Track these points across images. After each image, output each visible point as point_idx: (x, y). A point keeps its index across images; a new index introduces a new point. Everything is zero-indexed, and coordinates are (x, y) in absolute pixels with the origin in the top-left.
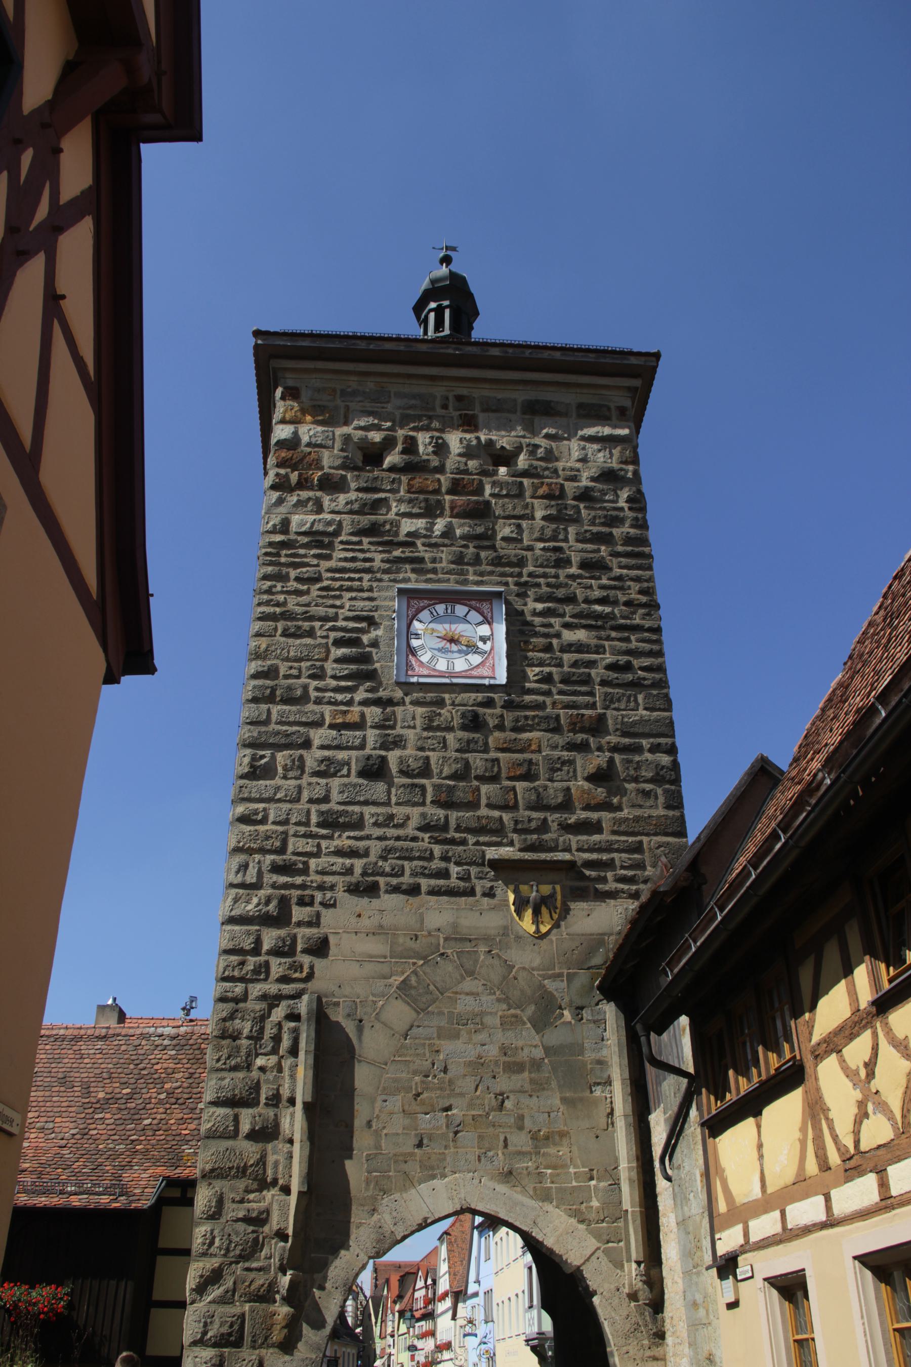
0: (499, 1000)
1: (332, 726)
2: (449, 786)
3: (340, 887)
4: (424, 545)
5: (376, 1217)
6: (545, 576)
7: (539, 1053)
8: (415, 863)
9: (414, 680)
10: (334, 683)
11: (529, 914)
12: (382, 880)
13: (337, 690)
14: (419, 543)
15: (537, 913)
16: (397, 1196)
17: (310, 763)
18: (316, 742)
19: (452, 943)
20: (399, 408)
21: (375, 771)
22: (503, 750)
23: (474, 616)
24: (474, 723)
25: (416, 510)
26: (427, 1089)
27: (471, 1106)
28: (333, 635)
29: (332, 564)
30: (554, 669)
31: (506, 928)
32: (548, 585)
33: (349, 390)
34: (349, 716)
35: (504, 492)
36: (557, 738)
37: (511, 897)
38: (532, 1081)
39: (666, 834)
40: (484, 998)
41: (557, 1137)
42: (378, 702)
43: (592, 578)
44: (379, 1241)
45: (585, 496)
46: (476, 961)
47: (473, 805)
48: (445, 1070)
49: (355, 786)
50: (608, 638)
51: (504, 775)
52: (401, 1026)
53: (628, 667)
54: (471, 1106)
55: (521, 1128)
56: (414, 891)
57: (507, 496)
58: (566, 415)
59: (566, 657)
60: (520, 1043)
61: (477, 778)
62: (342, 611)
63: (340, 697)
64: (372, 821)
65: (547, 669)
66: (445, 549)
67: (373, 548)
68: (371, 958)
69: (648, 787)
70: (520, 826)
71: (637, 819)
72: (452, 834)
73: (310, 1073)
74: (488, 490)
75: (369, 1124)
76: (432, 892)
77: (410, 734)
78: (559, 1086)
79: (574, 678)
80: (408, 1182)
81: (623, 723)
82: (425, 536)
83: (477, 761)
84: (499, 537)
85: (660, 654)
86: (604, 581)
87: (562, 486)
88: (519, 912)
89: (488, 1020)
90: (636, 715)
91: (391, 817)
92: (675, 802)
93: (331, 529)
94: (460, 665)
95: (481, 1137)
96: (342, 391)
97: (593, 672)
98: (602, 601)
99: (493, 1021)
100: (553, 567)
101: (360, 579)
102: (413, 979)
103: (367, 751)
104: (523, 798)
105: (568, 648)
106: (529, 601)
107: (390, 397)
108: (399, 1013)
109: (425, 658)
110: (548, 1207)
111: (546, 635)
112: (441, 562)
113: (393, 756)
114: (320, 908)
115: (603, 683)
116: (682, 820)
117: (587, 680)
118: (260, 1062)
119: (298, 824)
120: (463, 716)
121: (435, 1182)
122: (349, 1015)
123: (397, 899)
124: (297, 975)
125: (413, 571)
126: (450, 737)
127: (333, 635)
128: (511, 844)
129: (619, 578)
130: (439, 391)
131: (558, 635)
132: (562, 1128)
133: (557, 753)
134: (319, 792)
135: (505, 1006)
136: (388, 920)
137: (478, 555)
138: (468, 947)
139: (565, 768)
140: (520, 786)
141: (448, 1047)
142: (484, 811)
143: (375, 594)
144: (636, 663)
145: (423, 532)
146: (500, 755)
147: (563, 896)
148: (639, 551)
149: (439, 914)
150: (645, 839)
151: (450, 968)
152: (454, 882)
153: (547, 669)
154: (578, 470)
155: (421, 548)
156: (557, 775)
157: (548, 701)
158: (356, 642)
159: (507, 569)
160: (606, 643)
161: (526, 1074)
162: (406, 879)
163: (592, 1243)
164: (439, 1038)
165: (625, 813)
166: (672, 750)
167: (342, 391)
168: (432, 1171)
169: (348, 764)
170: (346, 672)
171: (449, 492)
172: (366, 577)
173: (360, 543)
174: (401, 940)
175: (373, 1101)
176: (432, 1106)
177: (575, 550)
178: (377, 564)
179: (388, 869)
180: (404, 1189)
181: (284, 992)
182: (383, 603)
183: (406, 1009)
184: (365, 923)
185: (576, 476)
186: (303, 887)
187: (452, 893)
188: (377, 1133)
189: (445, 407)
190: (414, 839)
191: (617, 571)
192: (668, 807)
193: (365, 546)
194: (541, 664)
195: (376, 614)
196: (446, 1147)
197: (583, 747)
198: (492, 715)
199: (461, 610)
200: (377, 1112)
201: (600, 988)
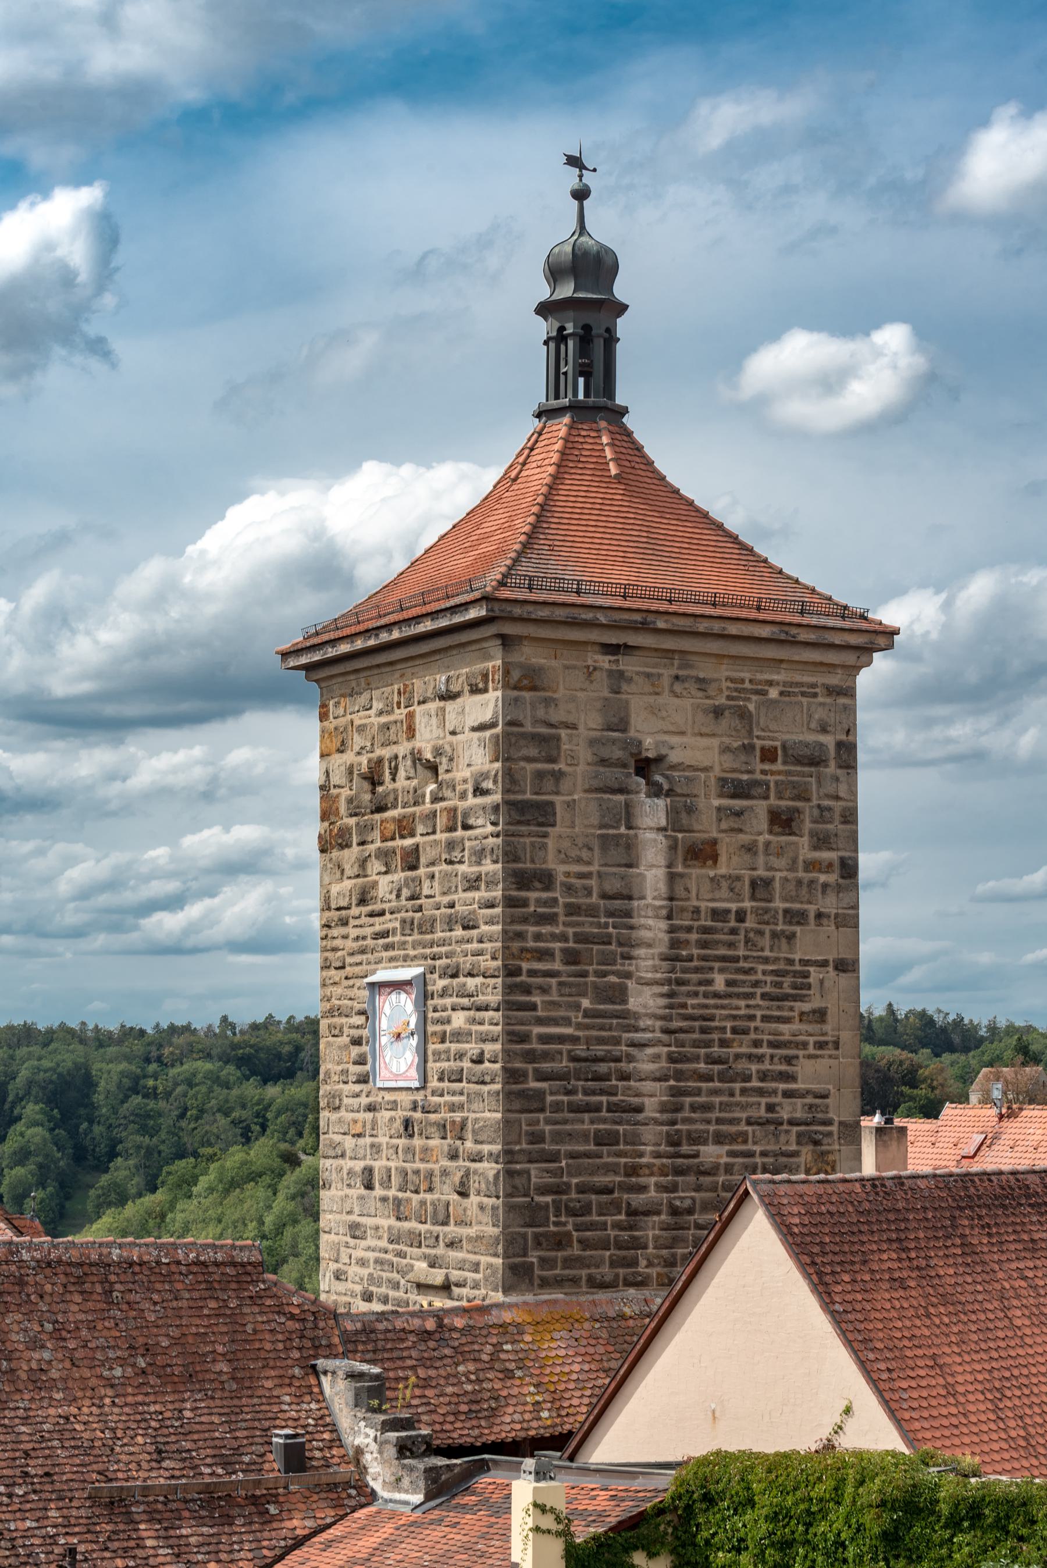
29: (350, 944)
42: (371, 1108)
66: (398, 916)
69: (486, 1200)
140: (428, 1197)
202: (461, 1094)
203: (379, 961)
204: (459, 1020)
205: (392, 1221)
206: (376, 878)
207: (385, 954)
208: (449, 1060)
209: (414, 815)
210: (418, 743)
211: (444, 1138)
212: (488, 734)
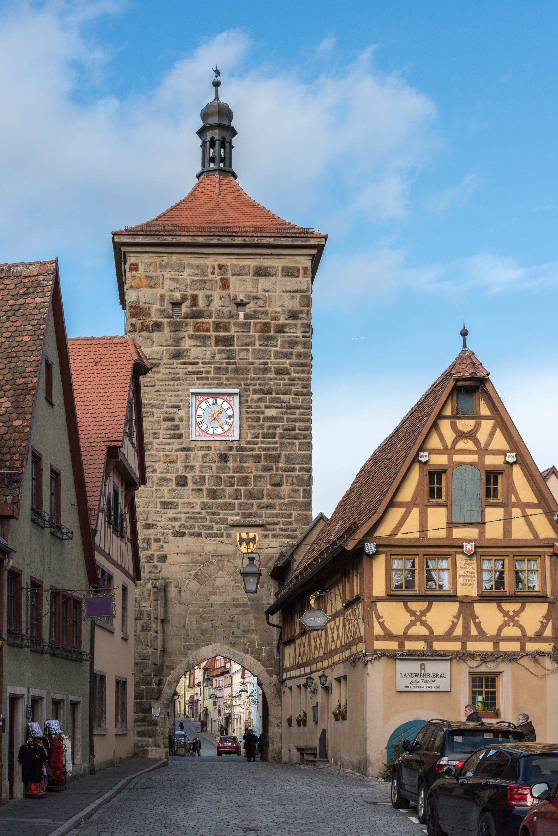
0: (232, 580)
1: (164, 462)
2: (213, 489)
3: (170, 534)
4: (203, 363)
5: (187, 658)
6: (259, 379)
7: (246, 601)
8: (200, 524)
9: (199, 439)
10: (165, 440)
11: (244, 545)
12: (187, 531)
13: (165, 444)
14: (200, 361)
15: (248, 544)
16: (194, 651)
17: (155, 480)
18: (158, 471)
19: (214, 557)
20: (190, 275)
21: (182, 481)
22: (236, 472)
23: (226, 405)
24: (224, 458)
25: (199, 344)
26: (205, 614)
27: (221, 620)
28: (162, 416)
29: (160, 376)
30: (261, 431)
31: (235, 551)
32: (260, 385)
33: (163, 263)
34: (171, 458)
35: (242, 330)
36: (260, 465)
37: (238, 538)
38: (243, 611)
39: (302, 510)
40: (226, 579)
41: (252, 632)
42: (183, 450)
43: (281, 380)
44: (188, 666)
45: (281, 329)
46: (224, 564)
47: (223, 497)
48: (212, 607)
49: (175, 490)
50: (286, 413)
51: (236, 484)
52: (195, 590)
53: (294, 429)
54: (221, 620)
55: (239, 628)
56: (199, 535)
57: (242, 332)
59: (266, 424)
60: (240, 597)
61: (225, 486)
62: (166, 403)
63: (167, 448)
64: (182, 506)
65: (257, 431)
66: (213, 366)
67: (180, 366)
68: (184, 564)
69: (297, 488)
70: (242, 508)
71: (291, 503)
72: (214, 511)
73: (162, 610)
74: (233, 329)
75: (184, 626)
76: (207, 536)
77: (197, 465)
78: (253, 613)
79: (269, 436)
80: (198, 647)
81: (289, 458)
82: (203, 359)
84: (237, 358)
85: (309, 421)
86: (287, 382)
87: (269, 324)
89: (228, 588)
90: (294, 454)
91: (190, 503)
92: (308, 493)
93: (159, 356)
94: (219, 431)
95: (224, 631)
96: (160, 264)
97: (278, 431)
98: (285, 393)
99: (230, 589)
100: (263, 374)
101: (173, 385)
102: (200, 572)
103: (179, 474)
104: (244, 495)
106: (251, 393)
107: (184, 268)
108: (194, 585)
109: (203, 428)
110: (248, 656)
111: (258, 413)
112: (210, 374)
113: (189, 476)
114: (163, 544)
115: (282, 437)
116: (310, 504)
117: (273, 436)
118: (144, 605)
119: (154, 508)
120: (221, 455)
121: (208, 647)
122: (176, 587)
123: (193, 539)
124: (156, 571)
125: (198, 379)
126: (214, 465)
127: (162, 416)
128: (238, 514)
129: (293, 379)
130: (209, 262)
131: (263, 412)
132: (254, 628)
133: (259, 473)
134: (160, 494)
135: (234, 582)
136: (190, 549)
137: (227, 369)
138: (220, 559)
139: (262, 481)
140: (242, 488)
141: (212, 597)
142: (227, 500)
143: (180, 393)
144: (297, 425)
145: (203, 356)
146: (235, 475)
147: (259, 538)
148: (305, 363)
149: (209, 545)
150: (294, 512)
151: (213, 567)
152: (215, 531)
153: (257, 431)
154: (278, 312)
155: (200, 365)
156: (259, 483)
157: (256, 446)
158: (173, 420)
159: (241, 376)
160: (285, 416)
161: (241, 609)
162: (196, 530)
163: (262, 668)
164: (209, 594)
165: (286, 501)
166: (309, 470)
167: (160, 264)
168: (207, 643)
169: (172, 480)
170: (169, 436)
171: (214, 331)
172: (176, 383)
173: (173, 364)
174: (195, 556)
175: (185, 618)
176: (207, 619)
177: (273, 362)
178: (180, 375)
179: (189, 527)
180: (197, 649)
181: (151, 578)
182: (184, 398)
183: (197, 583)
184: (181, 550)
185: (277, 317)
186: (156, 534)
187: (214, 536)
188: (187, 630)
189: (213, 273)
190: (199, 513)
191: (293, 375)
192: (304, 497)
193: (175, 365)
194: (254, 427)
195: (181, 404)
196: (212, 634)
197: (271, 469)
198: (233, 455)
199: (219, 401)
200: (187, 622)
201: (271, 575)
202: (276, 443)
203: (194, 384)
204: (272, 412)
205: (206, 500)
206: (190, 348)
207: (197, 382)
208: (263, 429)
209: (229, 323)
210: (232, 291)
211: (259, 462)
212: (298, 295)
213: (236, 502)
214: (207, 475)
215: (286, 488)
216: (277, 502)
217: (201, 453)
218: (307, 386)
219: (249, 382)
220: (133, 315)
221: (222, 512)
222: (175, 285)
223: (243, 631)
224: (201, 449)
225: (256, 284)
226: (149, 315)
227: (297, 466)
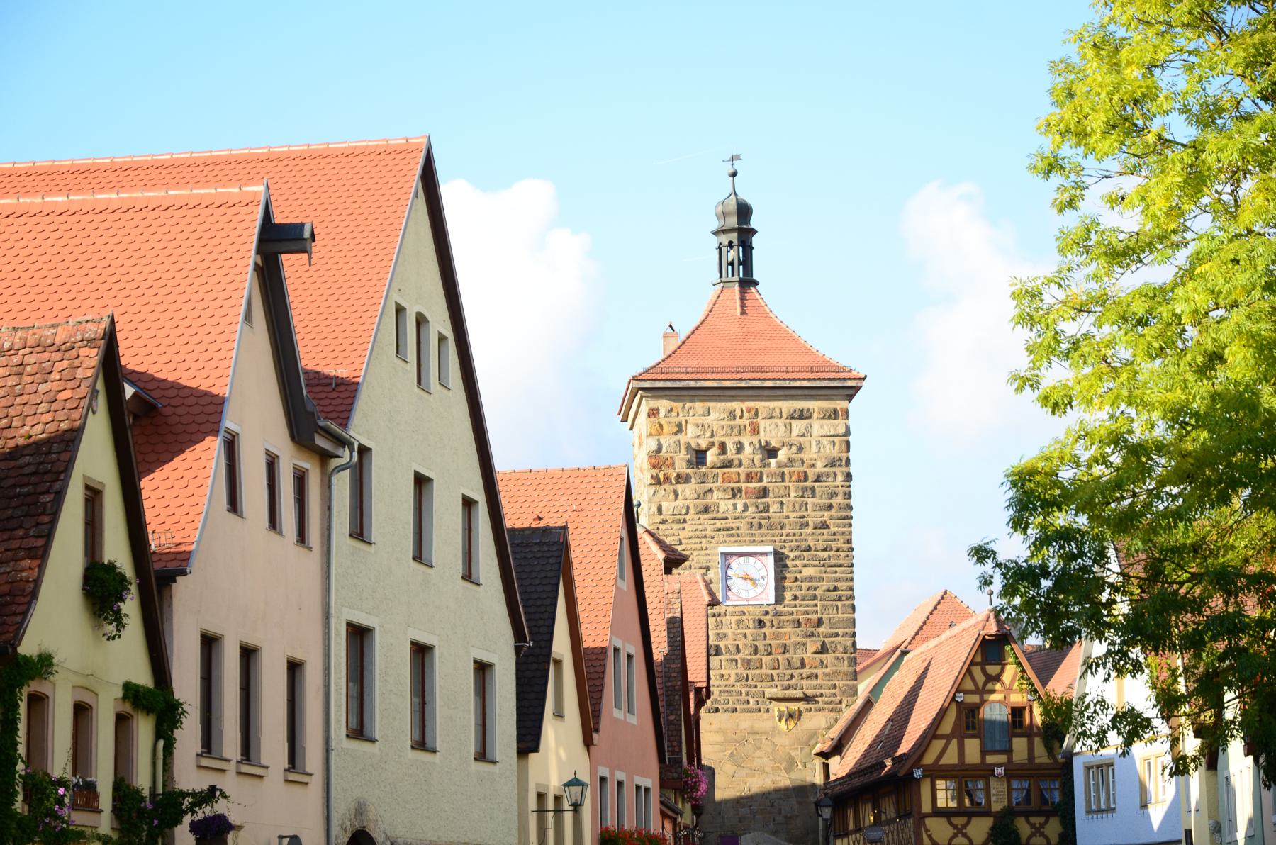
23: (759, 564)
56: (735, 710)
58: (810, 417)
59: (804, 584)
76: (743, 711)
77: (729, 632)
83: (761, 644)
88: (780, 720)
97: (817, 592)
98: (825, 550)
105: (805, 579)
130: (737, 405)
133: (798, 640)
140: (780, 657)
142: (763, 671)
162: (731, 705)
172: (704, 541)
184: (714, 727)
187: (750, 711)
191: (833, 529)
205: (742, 671)
212: (836, 439)
213: (774, 672)
214: (741, 643)
215: (829, 658)
216: (820, 671)
217: (734, 619)
218: (849, 542)
219: (784, 538)
220: (654, 467)
221: (759, 684)
222: (698, 432)
223: (785, 817)
224: (733, 614)
225: (789, 428)
226: (672, 466)
227: (840, 631)
